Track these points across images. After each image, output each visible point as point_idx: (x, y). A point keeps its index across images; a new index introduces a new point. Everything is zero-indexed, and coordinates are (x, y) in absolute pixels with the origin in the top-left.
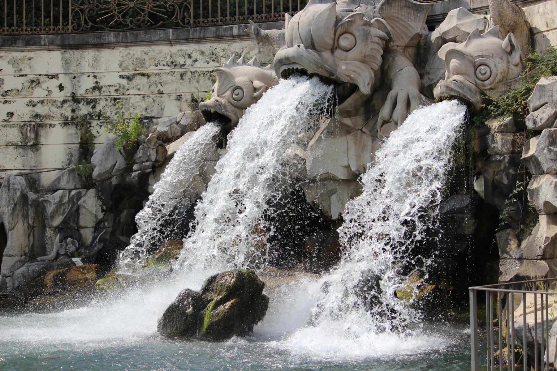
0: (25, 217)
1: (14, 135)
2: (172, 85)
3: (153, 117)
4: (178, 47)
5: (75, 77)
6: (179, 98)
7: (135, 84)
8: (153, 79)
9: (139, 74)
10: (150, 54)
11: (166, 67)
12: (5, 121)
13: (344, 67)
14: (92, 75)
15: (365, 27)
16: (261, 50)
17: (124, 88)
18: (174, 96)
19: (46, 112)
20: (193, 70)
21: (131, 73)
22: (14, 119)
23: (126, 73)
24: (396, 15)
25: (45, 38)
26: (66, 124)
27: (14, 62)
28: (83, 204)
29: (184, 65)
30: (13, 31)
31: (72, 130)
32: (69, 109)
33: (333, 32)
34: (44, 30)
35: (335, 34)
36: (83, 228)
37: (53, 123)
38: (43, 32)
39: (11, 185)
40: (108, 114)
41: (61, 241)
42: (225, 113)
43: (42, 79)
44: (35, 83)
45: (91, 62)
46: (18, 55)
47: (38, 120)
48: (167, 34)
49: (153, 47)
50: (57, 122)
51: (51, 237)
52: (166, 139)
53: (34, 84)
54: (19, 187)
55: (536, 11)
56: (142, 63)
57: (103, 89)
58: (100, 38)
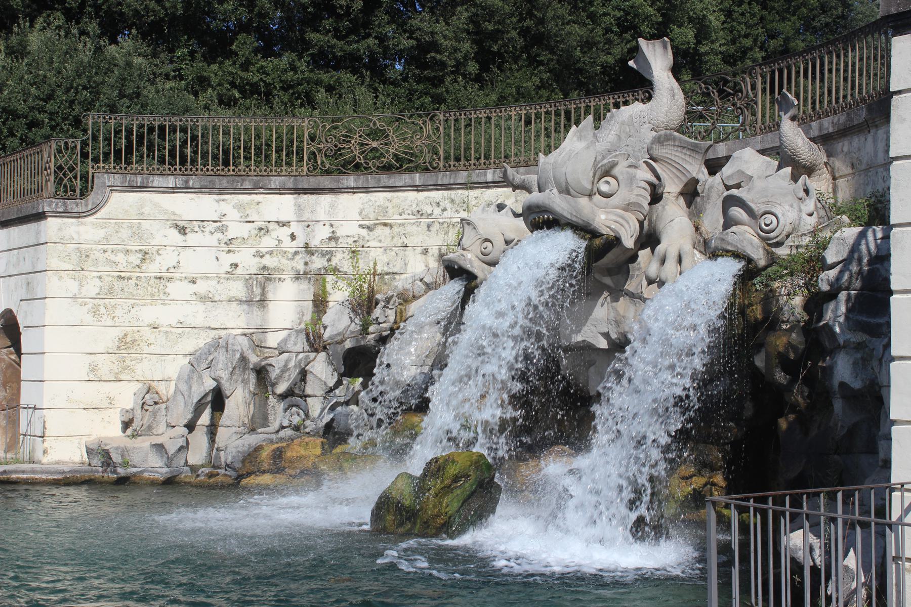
0: (245, 382)
1: (237, 289)
2: (418, 236)
3: (395, 274)
4: (425, 194)
5: (308, 226)
6: (425, 252)
7: (377, 235)
8: (396, 229)
9: (381, 224)
10: (393, 201)
11: (411, 217)
12: (228, 273)
13: (603, 217)
14: (328, 223)
15: (629, 170)
16: (518, 198)
17: (364, 239)
18: (419, 249)
19: (275, 264)
20: (441, 220)
21: (372, 222)
22: (239, 271)
23: (367, 223)
24: (668, 156)
25: (275, 181)
26: (297, 278)
27: (240, 207)
28: (311, 370)
29: (430, 215)
30: (240, 170)
32: (302, 262)
33: (591, 174)
34: (276, 171)
35: (594, 177)
36: (309, 396)
37: (283, 277)
38: (274, 173)
39: (230, 346)
40: (345, 269)
41: (285, 410)
42: (471, 269)
43: (271, 226)
44: (263, 230)
45: (327, 208)
47: (266, 272)
48: (412, 179)
49: (398, 194)
50: (288, 276)
51: (273, 406)
52: (406, 298)
53: (262, 232)
54: (239, 348)
55: (839, 149)
56: (385, 210)
57: (340, 240)
58: (338, 182)
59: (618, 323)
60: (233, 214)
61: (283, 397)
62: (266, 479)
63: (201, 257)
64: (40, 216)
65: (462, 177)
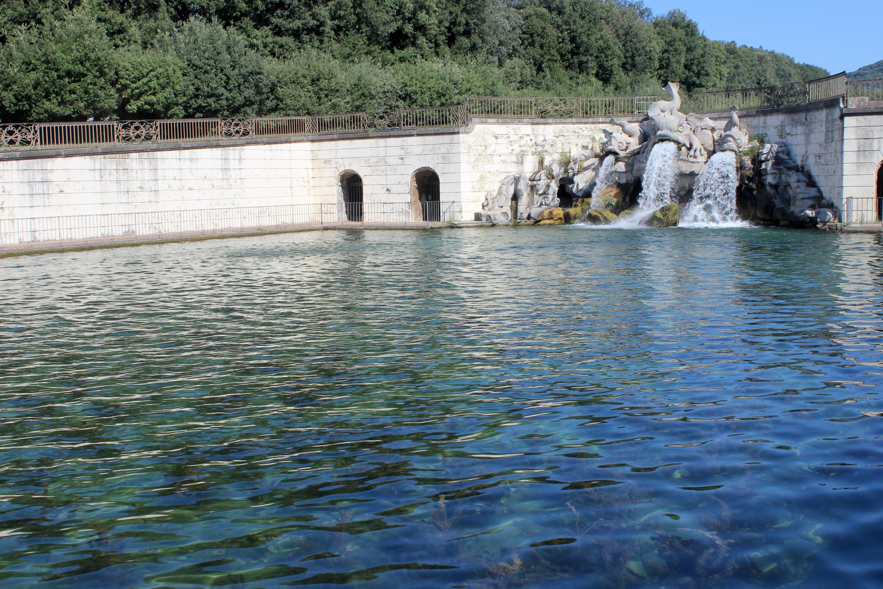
1: (514, 158)
2: (574, 140)
25: (526, 120)
27: (514, 129)
31: (535, 157)
46: (515, 126)
59: (678, 168)
60: (512, 132)
61: (541, 195)
62: (547, 222)
63: (502, 147)
64: (458, 133)
65: (590, 120)
